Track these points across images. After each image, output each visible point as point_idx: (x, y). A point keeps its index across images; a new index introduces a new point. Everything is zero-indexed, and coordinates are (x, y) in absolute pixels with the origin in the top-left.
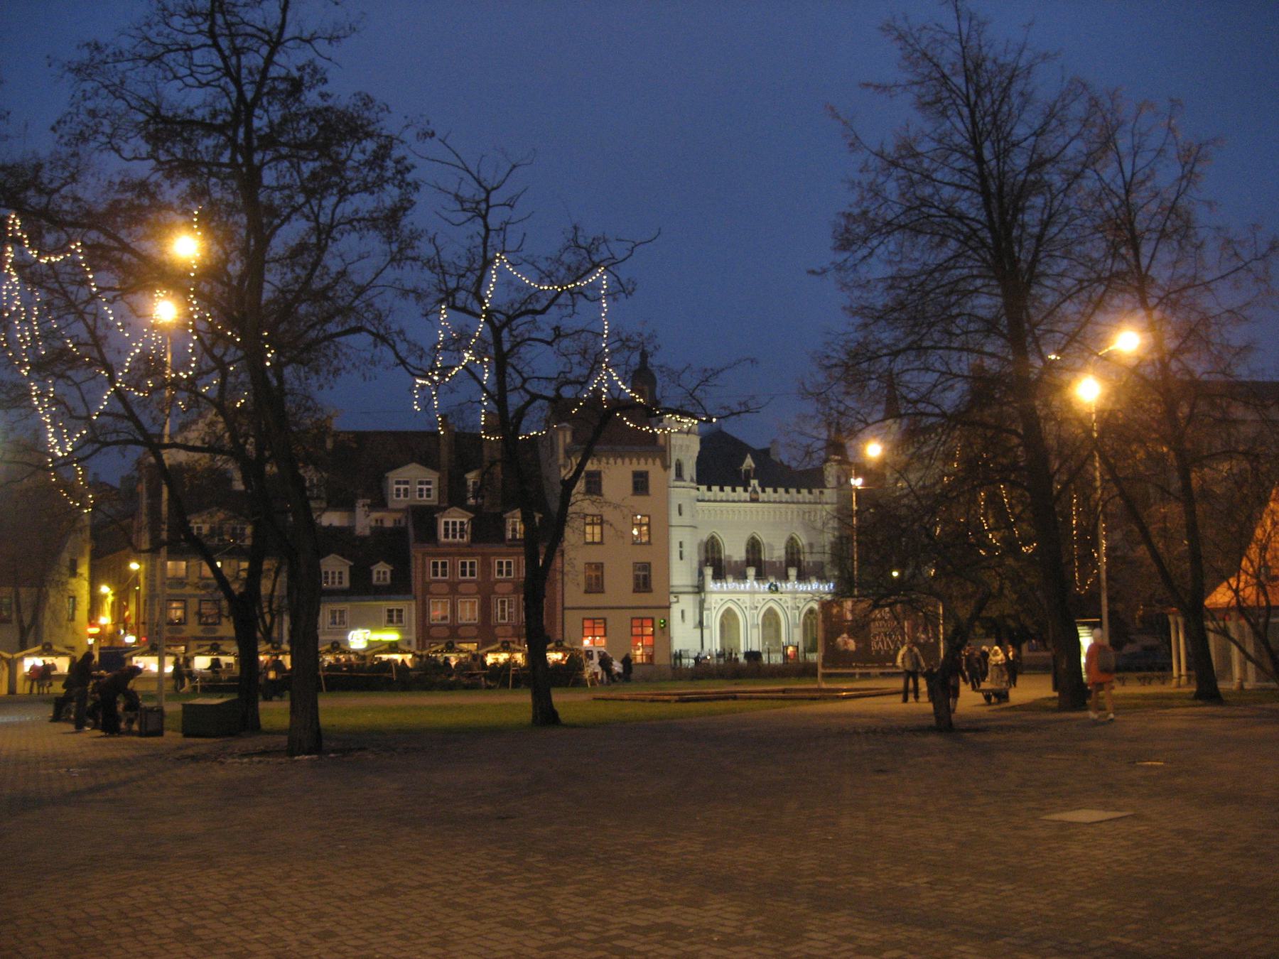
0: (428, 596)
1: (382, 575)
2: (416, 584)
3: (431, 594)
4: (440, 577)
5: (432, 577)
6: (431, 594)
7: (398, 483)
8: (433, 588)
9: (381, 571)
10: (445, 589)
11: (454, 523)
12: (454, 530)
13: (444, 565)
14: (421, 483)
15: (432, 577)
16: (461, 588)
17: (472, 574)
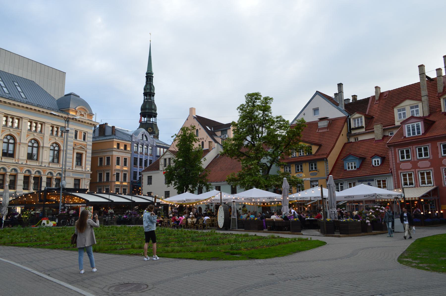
0: (399, 171)
1: (377, 163)
2: (392, 165)
3: (401, 169)
4: (405, 159)
5: (401, 160)
6: (401, 169)
7: (399, 110)
8: (401, 166)
9: (376, 161)
10: (409, 165)
11: (413, 127)
12: (413, 130)
13: (407, 152)
14: (412, 108)
15: (401, 160)
16: (420, 164)
17: (426, 154)
